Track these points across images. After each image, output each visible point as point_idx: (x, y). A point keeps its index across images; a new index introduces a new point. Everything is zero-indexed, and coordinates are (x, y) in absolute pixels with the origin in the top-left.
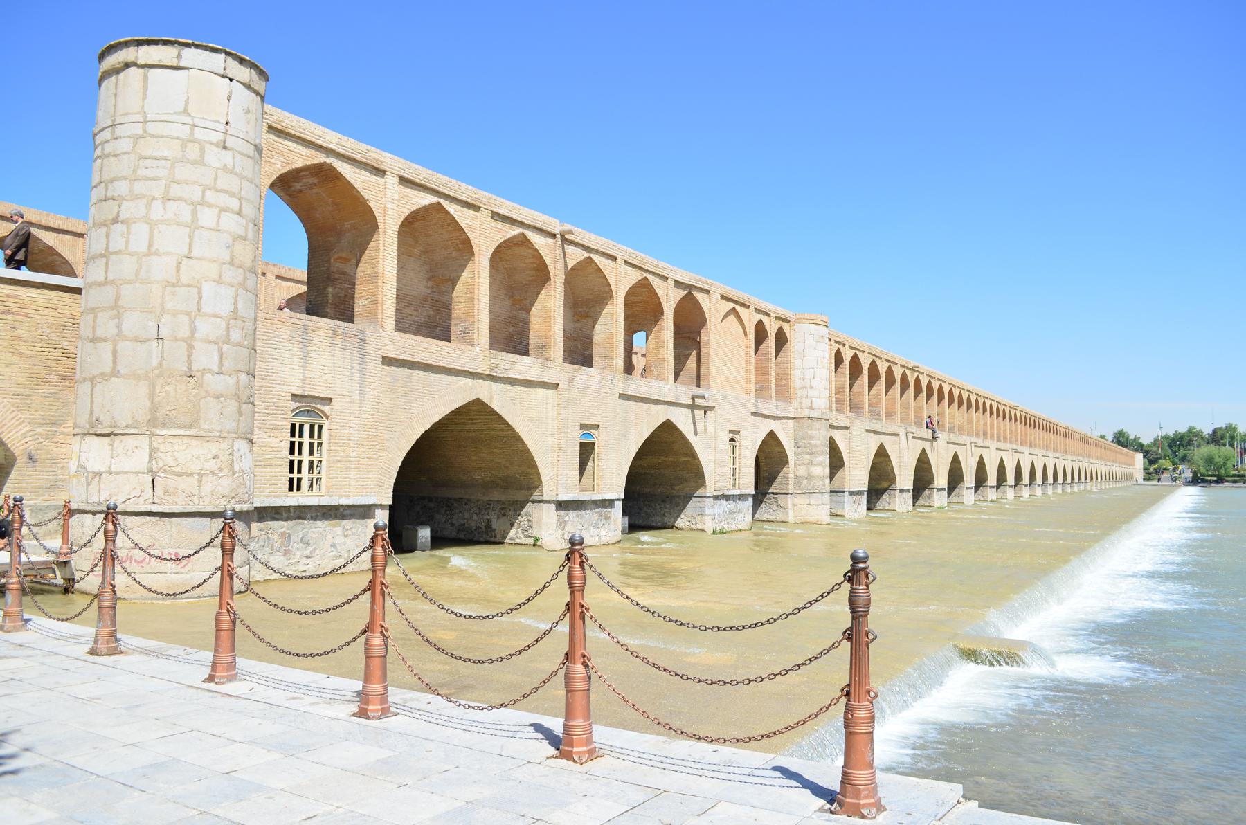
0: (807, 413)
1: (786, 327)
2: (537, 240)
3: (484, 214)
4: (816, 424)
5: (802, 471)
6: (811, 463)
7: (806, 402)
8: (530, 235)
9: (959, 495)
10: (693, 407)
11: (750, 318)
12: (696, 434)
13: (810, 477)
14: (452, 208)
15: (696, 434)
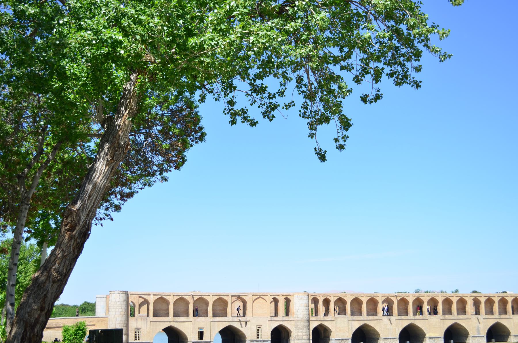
0: (297, 319)
1: (289, 297)
2: (185, 297)
3: (171, 297)
4: (300, 322)
5: (296, 334)
6: (298, 332)
7: (296, 316)
8: (184, 296)
9: (469, 340)
10: (240, 321)
11: (270, 299)
12: (242, 327)
13: (298, 336)
14: (164, 297)
15: (242, 327)
